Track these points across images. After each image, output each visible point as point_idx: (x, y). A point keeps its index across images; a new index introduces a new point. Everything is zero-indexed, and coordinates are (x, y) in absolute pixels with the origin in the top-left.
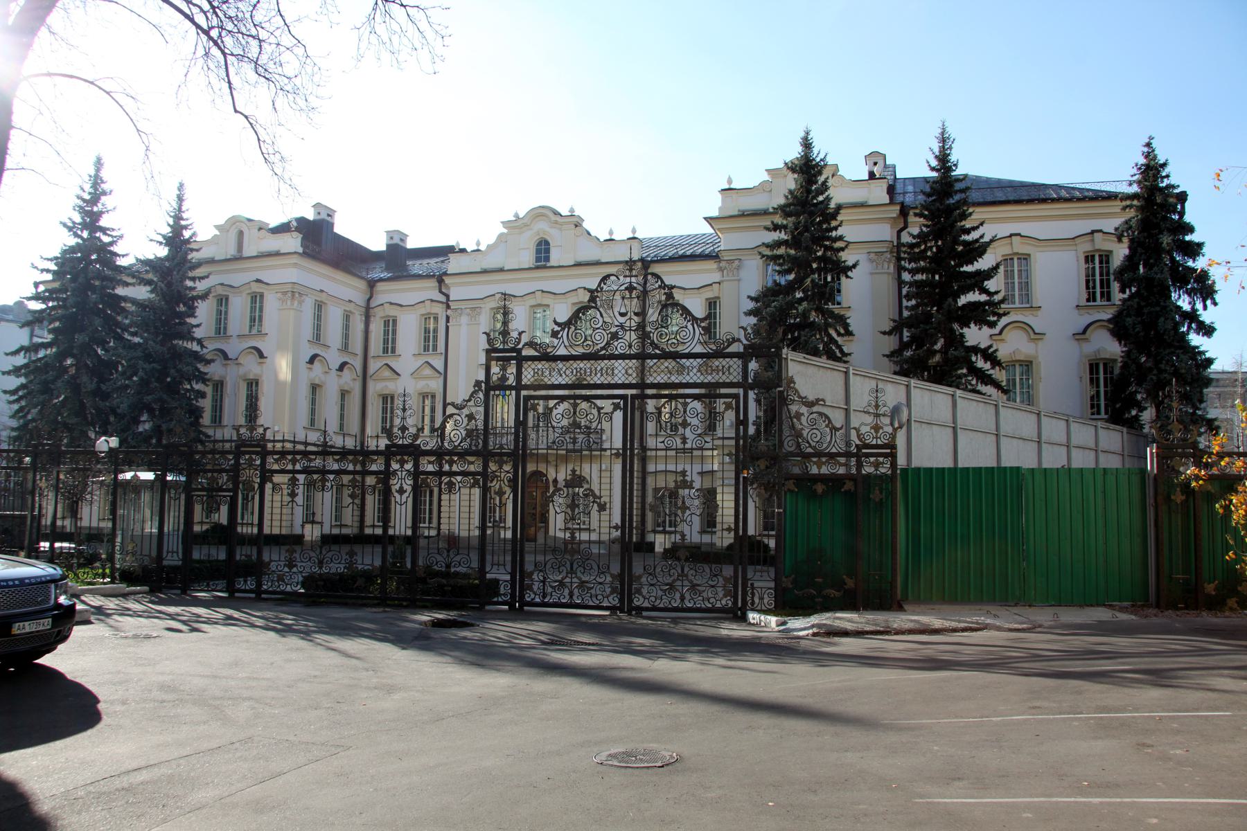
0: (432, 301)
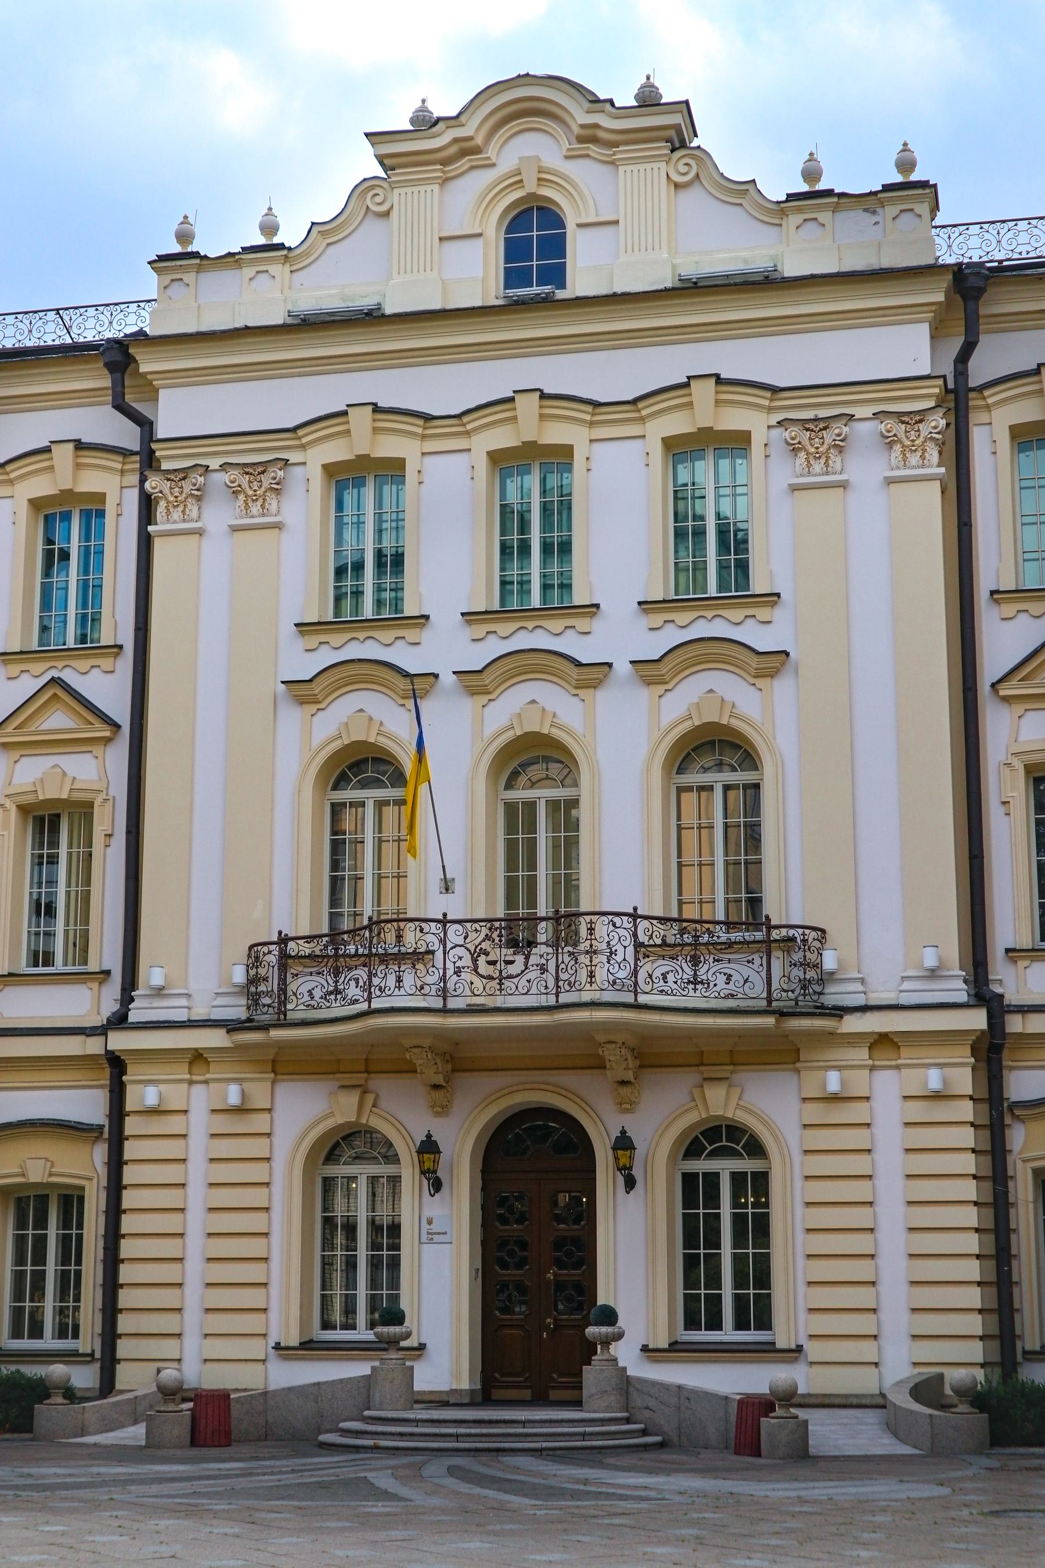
0: (80, 446)
